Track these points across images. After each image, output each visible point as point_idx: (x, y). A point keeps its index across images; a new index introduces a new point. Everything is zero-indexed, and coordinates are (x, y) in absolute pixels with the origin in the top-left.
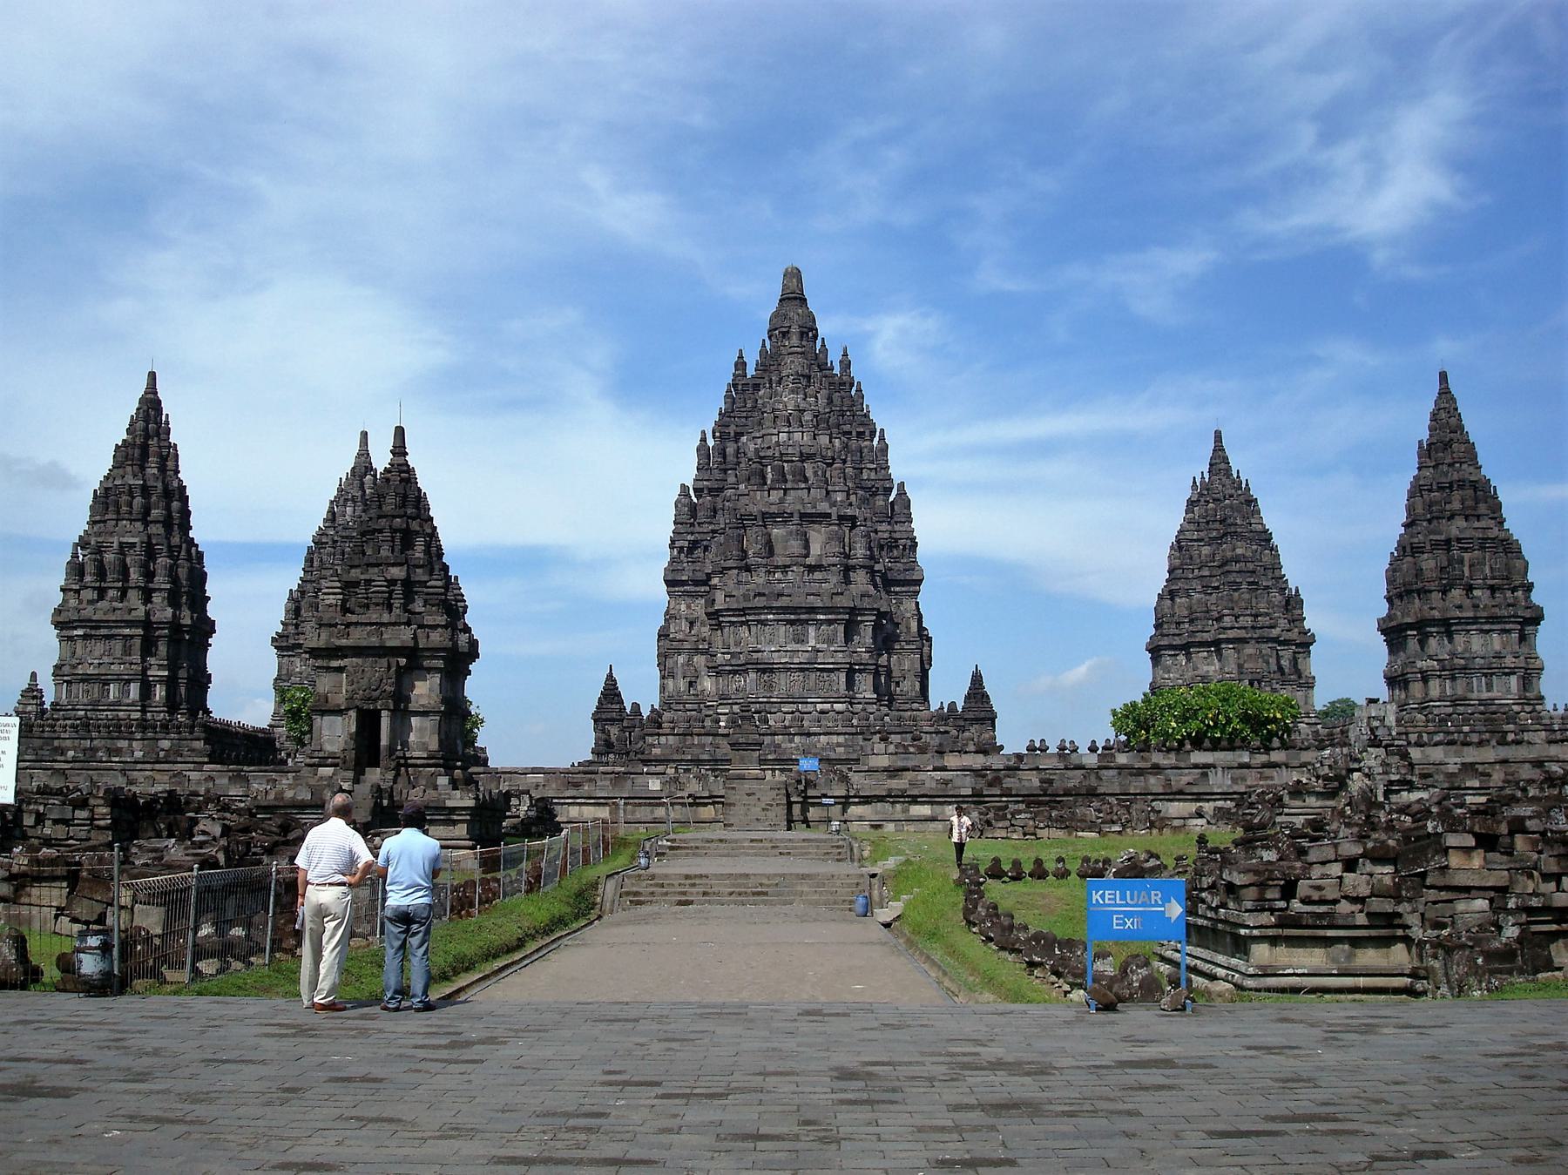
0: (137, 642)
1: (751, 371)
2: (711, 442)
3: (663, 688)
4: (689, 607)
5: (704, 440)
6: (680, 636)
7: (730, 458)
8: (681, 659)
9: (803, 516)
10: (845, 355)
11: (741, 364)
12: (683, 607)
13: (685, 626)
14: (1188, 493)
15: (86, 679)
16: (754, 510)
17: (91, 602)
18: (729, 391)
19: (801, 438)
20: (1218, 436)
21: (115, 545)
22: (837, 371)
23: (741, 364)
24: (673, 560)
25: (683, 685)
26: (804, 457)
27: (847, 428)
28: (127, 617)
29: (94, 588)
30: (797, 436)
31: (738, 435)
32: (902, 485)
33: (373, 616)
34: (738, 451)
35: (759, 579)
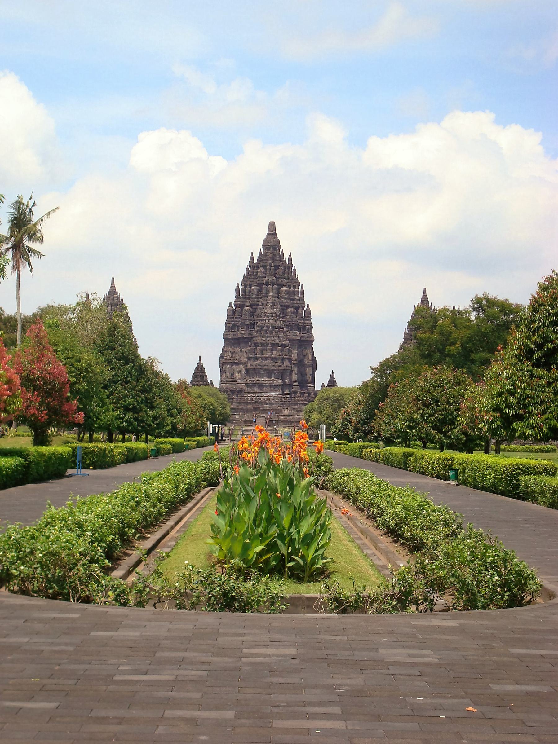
1: (256, 261)
2: (240, 287)
3: (221, 376)
5: (238, 286)
6: (228, 358)
7: (247, 294)
9: (272, 344)
10: (290, 256)
11: (252, 258)
13: (230, 354)
14: (412, 311)
16: (259, 341)
18: (247, 268)
19: (272, 322)
20: (425, 290)
22: (287, 262)
24: (226, 331)
25: (228, 375)
26: (274, 327)
27: (290, 284)
30: (271, 321)
31: (251, 286)
32: (308, 305)
34: (250, 292)
35: (260, 361)
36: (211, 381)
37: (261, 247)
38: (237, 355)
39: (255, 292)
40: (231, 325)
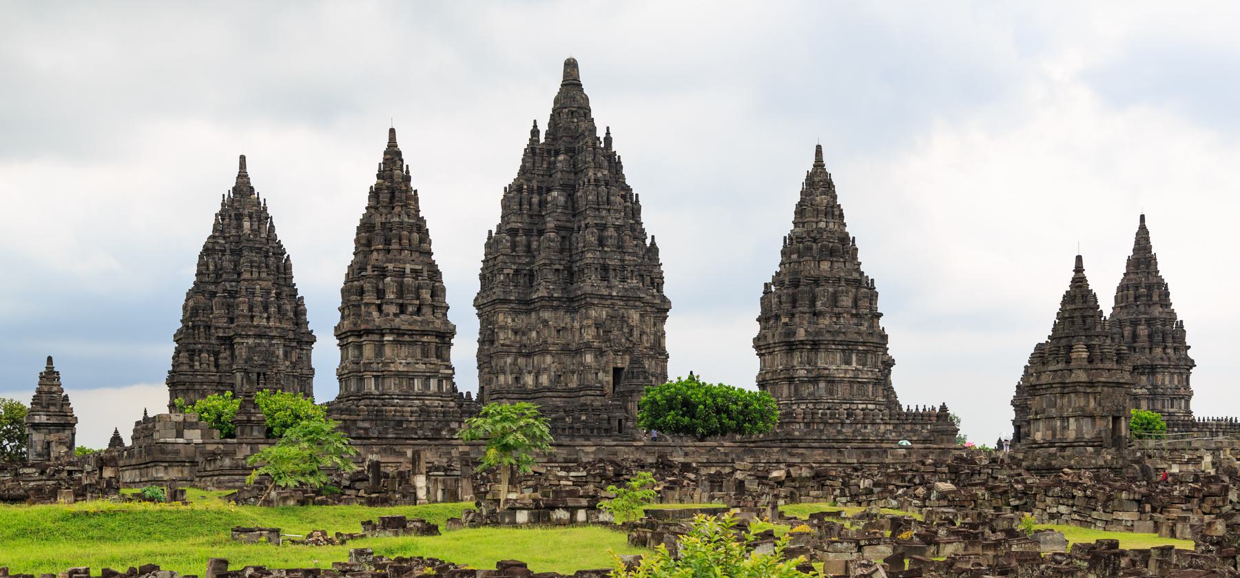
0: (433, 346)
1: (542, 140)
4: (513, 320)
6: (508, 342)
8: (509, 360)
9: (847, 280)
10: (608, 133)
12: (509, 320)
15: (398, 374)
17: (396, 315)
21: (408, 271)
25: (510, 379)
28: (427, 328)
29: (397, 304)
30: (831, 225)
33: (1109, 366)
34: (542, 203)
36: (469, 394)
38: (524, 338)
39: (562, 199)
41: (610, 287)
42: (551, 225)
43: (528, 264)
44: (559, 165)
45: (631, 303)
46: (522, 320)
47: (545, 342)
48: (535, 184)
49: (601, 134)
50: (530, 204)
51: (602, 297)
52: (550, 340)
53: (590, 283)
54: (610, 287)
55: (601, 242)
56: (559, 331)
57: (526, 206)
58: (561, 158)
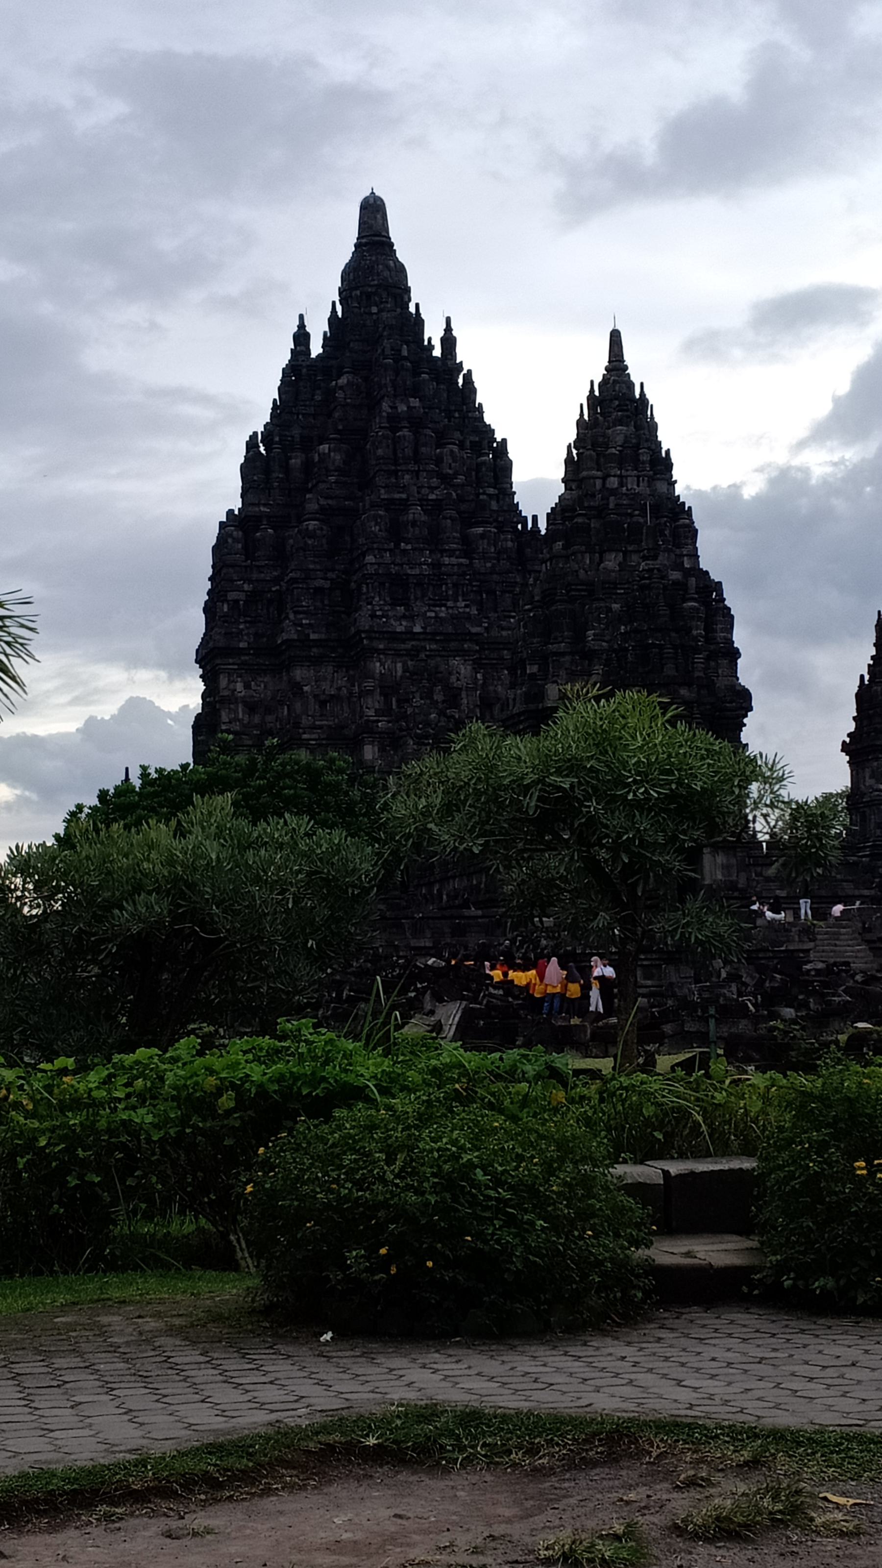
1: (316, 348)
11: (302, 337)
23: (302, 337)
31: (307, 444)
34: (308, 466)
37: (337, 299)
40: (242, 596)
41: (411, 618)
42: (312, 506)
43: (277, 580)
44: (340, 394)
45: (453, 645)
46: (264, 687)
47: (297, 725)
48: (296, 432)
49: (433, 332)
50: (286, 468)
51: (394, 637)
52: (305, 721)
53: (373, 612)
54: (411, 618)
55: (396, 532)
56: (323, 704)
57: (278, 474)
58: (343, 381)
